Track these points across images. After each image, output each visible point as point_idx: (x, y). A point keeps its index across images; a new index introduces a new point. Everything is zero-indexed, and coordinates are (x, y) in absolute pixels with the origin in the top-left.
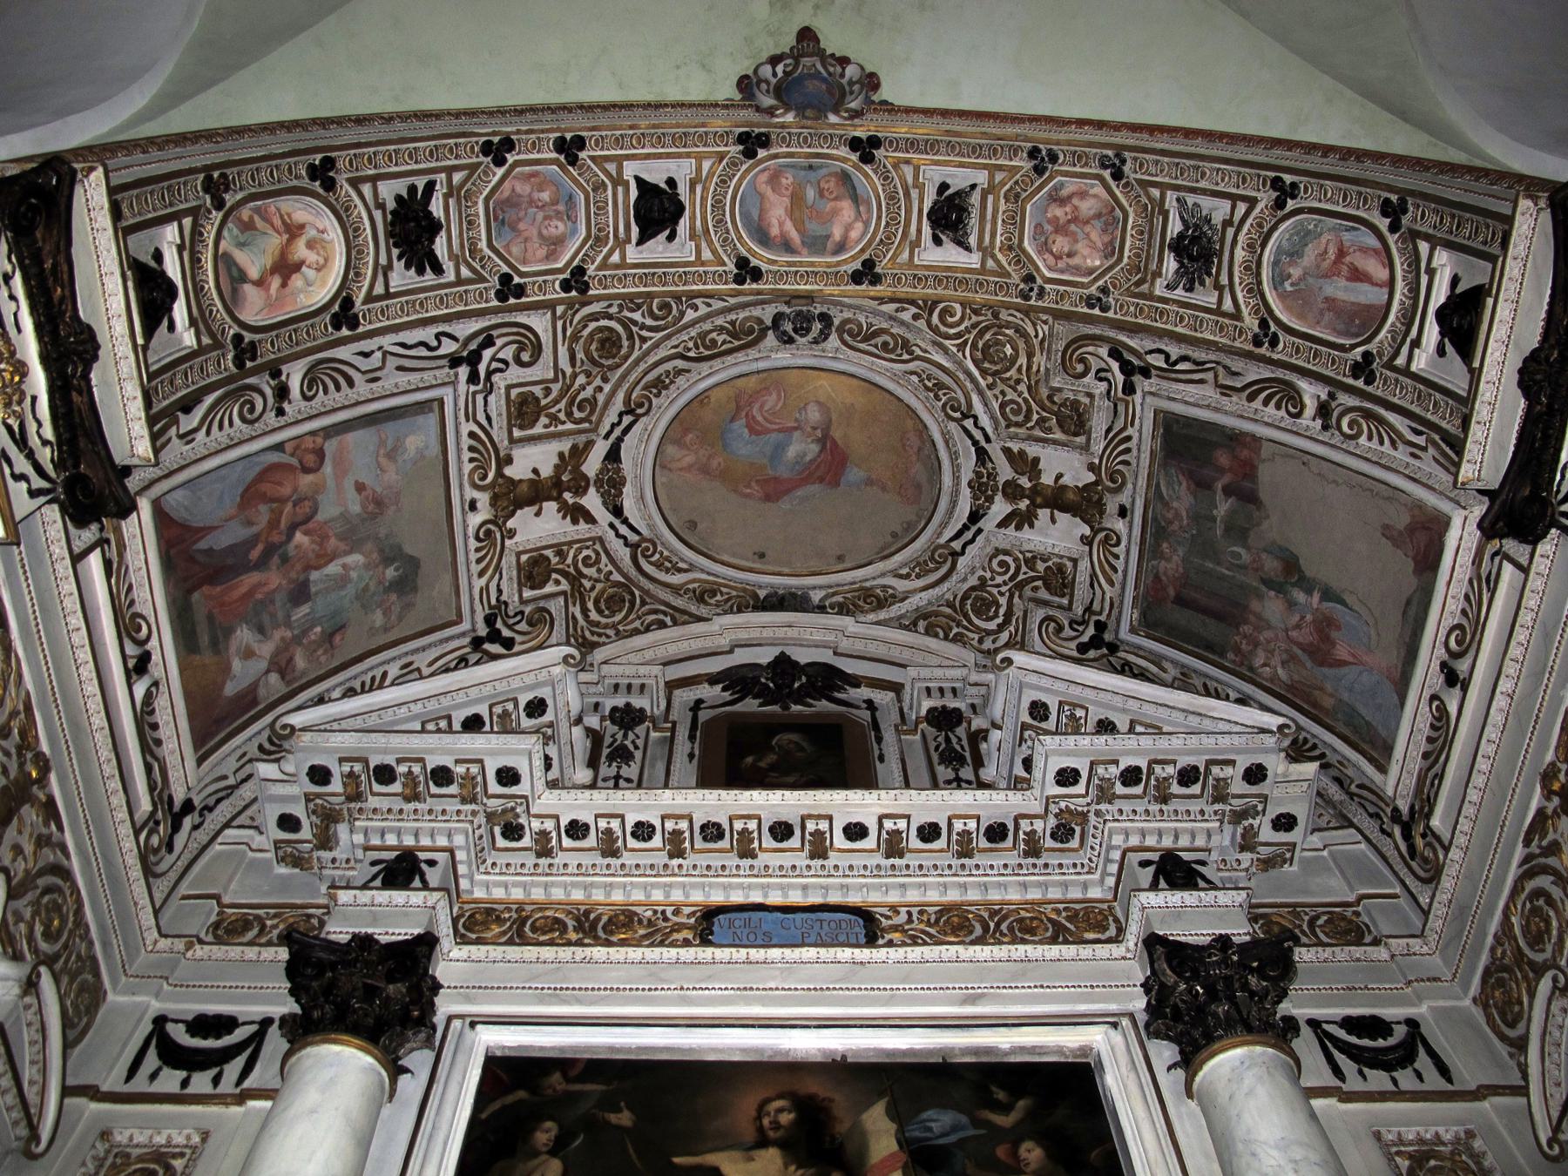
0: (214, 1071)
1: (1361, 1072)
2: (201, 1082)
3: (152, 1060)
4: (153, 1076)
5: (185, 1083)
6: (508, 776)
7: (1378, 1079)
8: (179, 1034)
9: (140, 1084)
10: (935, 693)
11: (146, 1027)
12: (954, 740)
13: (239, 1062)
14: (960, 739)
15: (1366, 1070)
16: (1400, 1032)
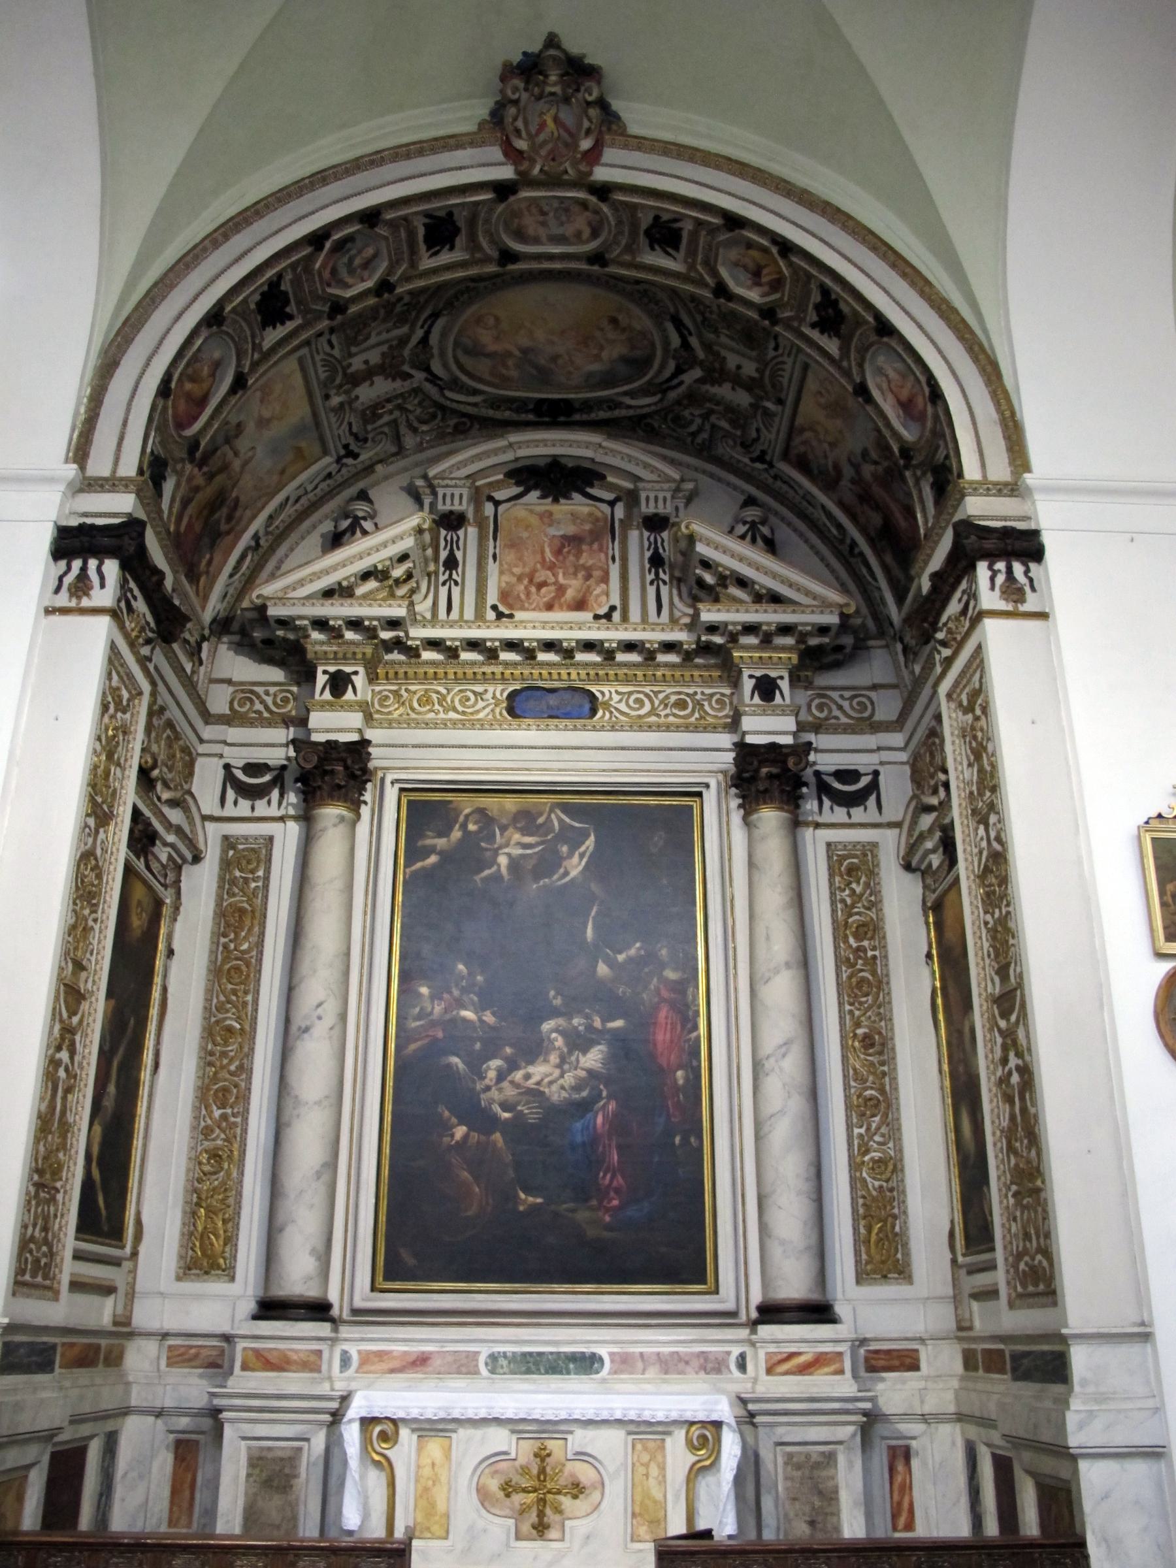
0: (266, 799)
1: (832, 809)
2: (262, 808)
3: (231, 794)
4: (236, 803)
5: (253, 808)
6: (393, 624)
7: (840, 814)
8: (239, 774)
9: (229, 811)
10: (652, 503)
11: (221, 773)
12: (659, 541)
13: (275, 794)
14: (663, 541)
15: (836, 808)
16: (864, 781)
